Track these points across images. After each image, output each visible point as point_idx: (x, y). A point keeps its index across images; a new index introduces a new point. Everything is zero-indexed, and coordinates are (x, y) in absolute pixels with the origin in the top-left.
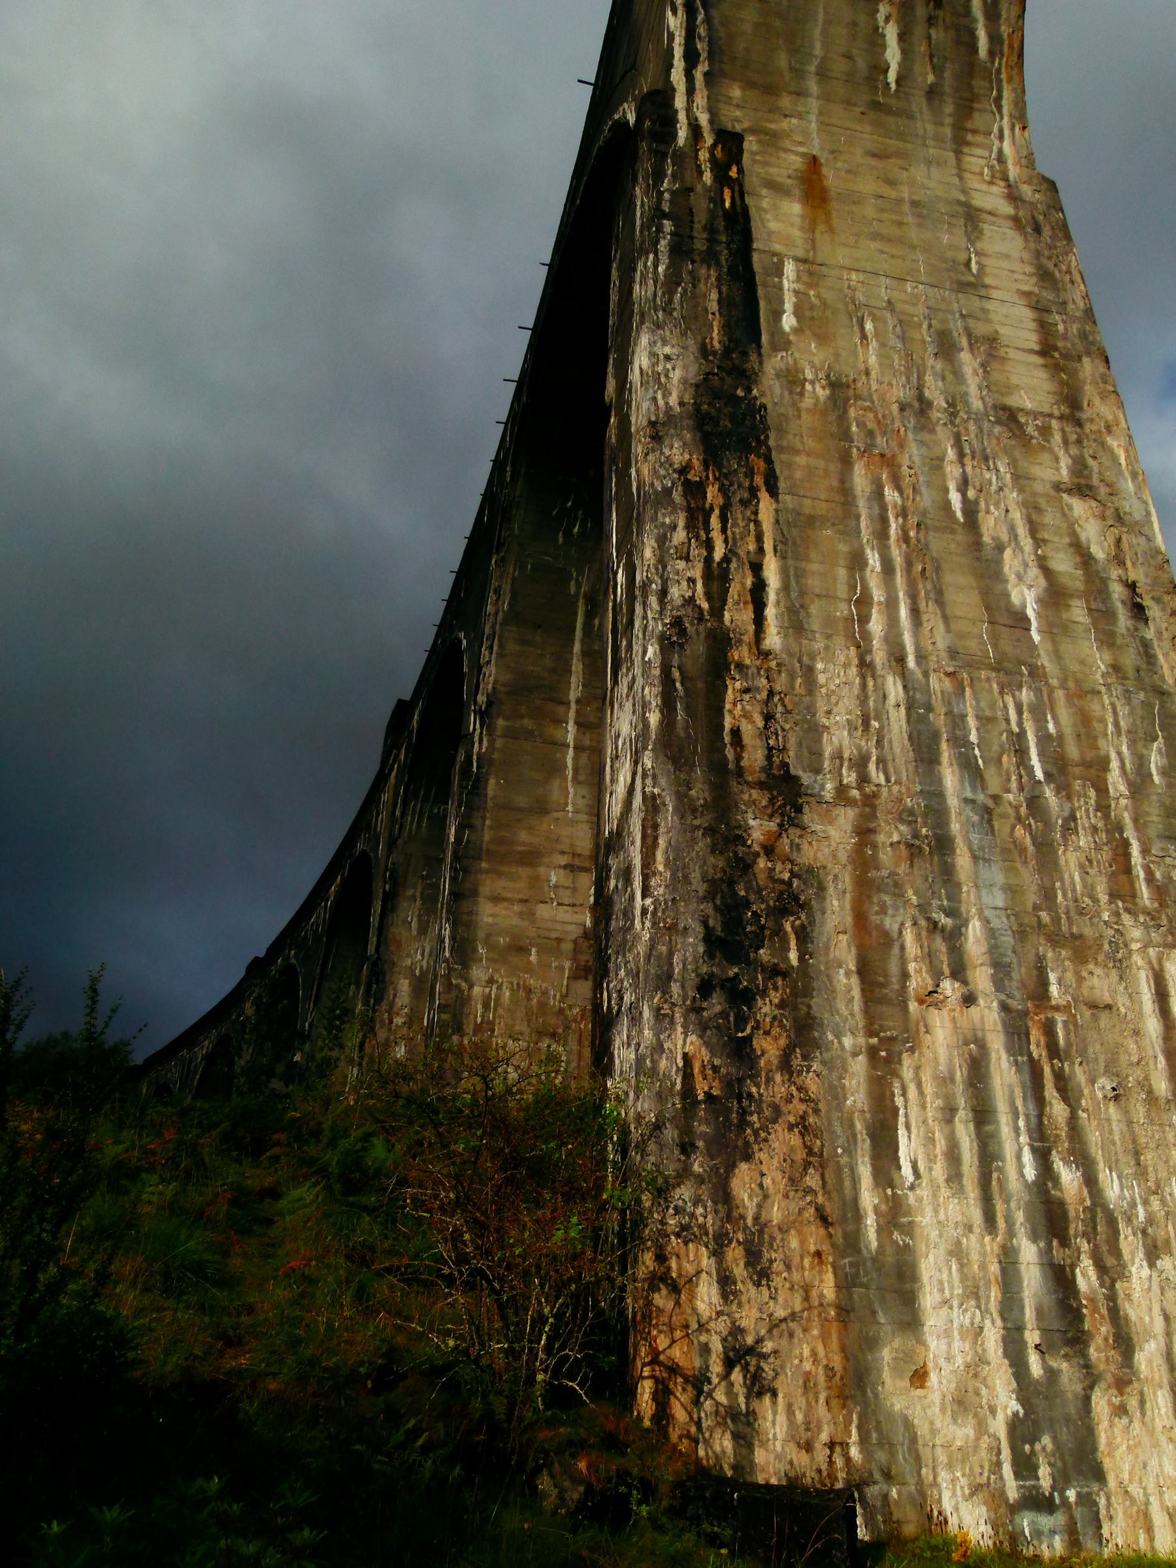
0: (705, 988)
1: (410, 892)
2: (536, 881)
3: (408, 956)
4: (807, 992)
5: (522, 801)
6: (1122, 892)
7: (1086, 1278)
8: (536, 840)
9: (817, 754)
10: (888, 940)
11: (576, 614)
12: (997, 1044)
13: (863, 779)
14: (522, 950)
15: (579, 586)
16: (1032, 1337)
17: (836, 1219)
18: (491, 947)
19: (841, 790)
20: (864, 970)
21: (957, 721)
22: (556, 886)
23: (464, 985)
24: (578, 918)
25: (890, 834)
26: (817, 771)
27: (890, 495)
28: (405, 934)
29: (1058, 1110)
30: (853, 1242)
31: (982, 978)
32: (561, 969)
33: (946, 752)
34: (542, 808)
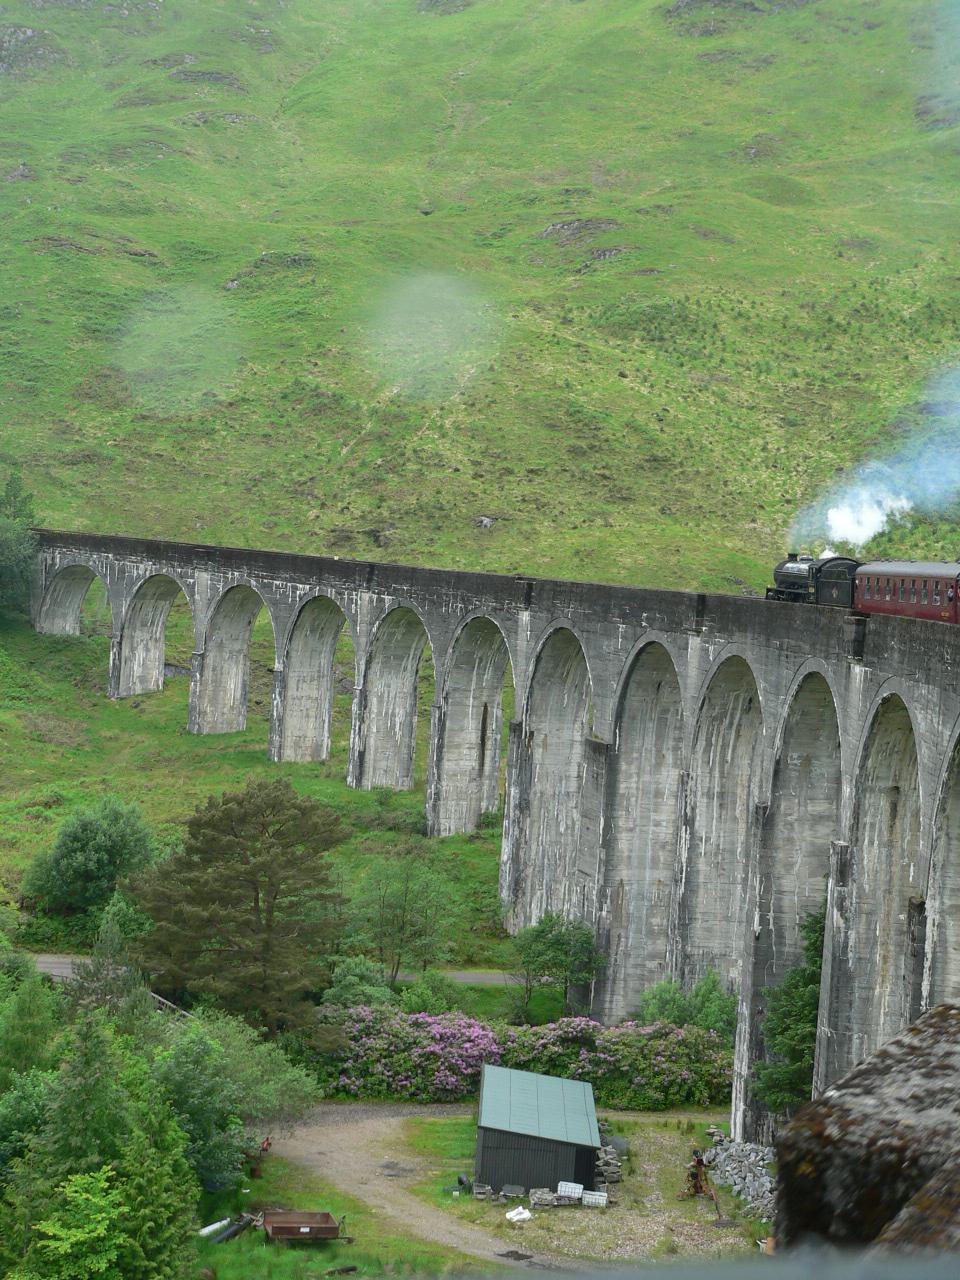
6: (564, 875)
17: (525, 913)
34: (462, 729)
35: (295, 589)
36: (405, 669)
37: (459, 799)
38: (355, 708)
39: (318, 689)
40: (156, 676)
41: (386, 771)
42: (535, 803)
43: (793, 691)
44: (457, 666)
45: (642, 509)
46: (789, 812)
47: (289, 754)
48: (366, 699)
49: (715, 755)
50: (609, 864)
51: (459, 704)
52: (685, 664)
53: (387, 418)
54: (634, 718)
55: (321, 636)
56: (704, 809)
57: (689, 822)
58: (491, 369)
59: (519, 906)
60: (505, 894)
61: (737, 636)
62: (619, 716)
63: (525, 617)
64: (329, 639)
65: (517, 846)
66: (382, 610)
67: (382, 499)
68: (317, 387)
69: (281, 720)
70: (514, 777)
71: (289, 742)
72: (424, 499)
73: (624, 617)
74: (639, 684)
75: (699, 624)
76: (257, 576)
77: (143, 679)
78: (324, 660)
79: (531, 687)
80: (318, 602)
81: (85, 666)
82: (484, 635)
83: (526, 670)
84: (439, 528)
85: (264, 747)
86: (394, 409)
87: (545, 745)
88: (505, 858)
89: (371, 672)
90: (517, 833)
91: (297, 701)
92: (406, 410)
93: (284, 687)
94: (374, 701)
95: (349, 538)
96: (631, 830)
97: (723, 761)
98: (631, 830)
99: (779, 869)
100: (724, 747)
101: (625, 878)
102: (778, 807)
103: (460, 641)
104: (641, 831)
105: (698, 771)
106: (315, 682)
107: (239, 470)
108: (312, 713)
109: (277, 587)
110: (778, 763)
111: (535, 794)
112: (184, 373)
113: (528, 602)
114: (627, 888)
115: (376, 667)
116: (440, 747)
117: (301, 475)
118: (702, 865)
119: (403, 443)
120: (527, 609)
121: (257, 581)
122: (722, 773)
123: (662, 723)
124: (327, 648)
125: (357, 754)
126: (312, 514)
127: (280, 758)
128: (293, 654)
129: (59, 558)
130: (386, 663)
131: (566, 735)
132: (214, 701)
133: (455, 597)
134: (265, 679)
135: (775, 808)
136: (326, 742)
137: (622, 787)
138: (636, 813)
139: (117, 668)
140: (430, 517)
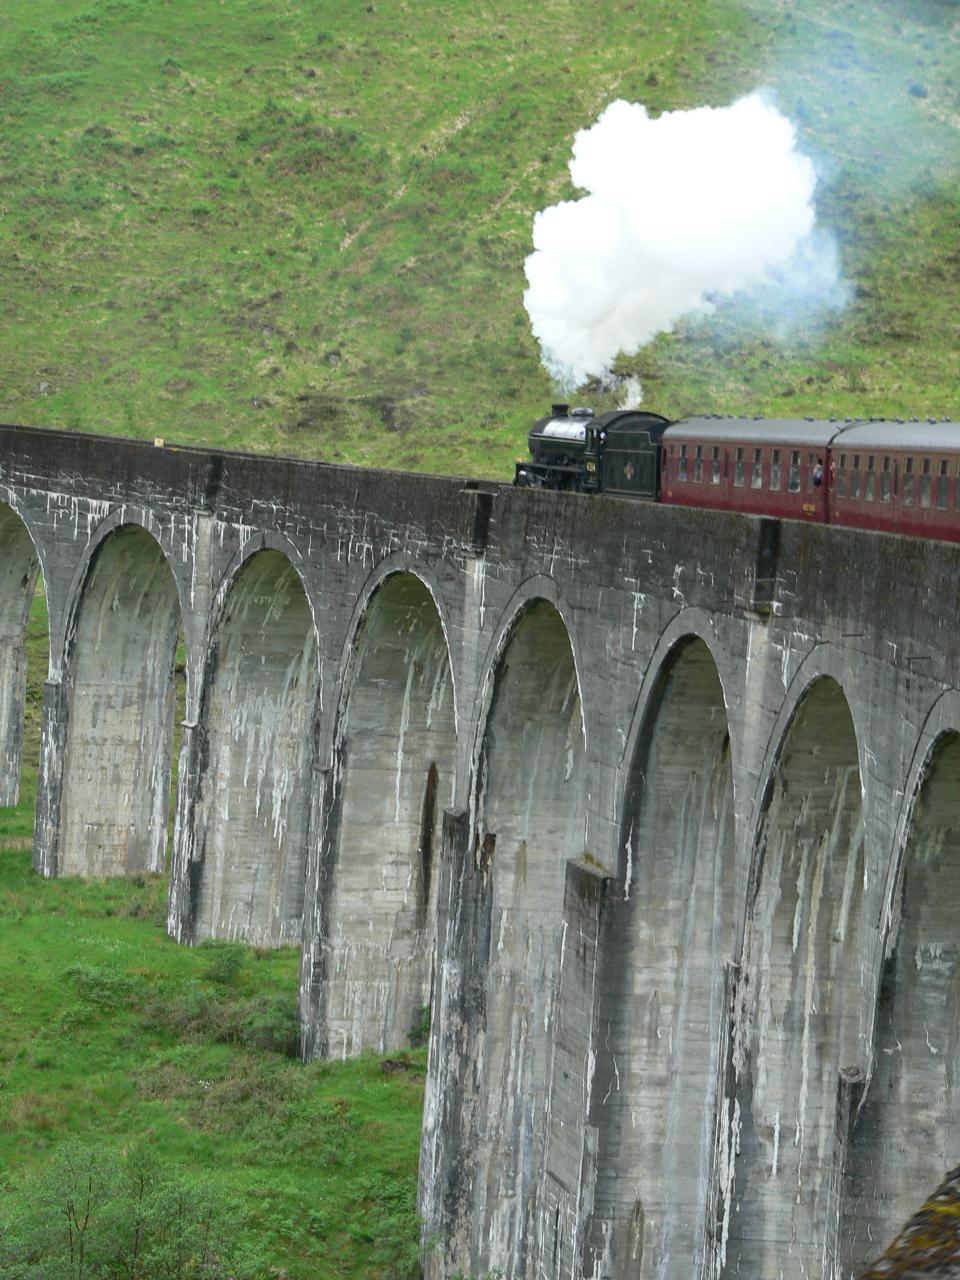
0: (448, 1196)
1: (229, 665)
2: (372, 875)
3: (229, 722)
4: (472, 1196)
5: (365, 817)
7: (529, 1260)
8: (373, 845)
9: (485, 1126)
10: (496, 1181)
11: (407, 675)
12: (519, 1207)
13: (497, 1132)
14: (363, 923)
15: (410, 657)
16: (513, 1273)
17: (473, 1252)
18: (345, 923)
19: (491, 1137)
20: (489, 1188)
21: (529, 1110)
22: (386, 878)
23: (329, 949)
24: (400, 898)
25: (501, 1150)
26: (484, 1132)
27: (524, 1024)
28: (224, 702)
29: (531, 1222)
30: (476, 1254)
31: (519, 1190)
32: (388, 933)
33: (523, 1122)
34: (378, 822)
35: (85, 508)
36: (294, 683)
37: (370, 976)
39: (140, 723)
41: (250, 905)
42: (498, 998)
43: (915, 781)
44: (363, 680)
45: (931, 356)
46: (919, 1099)
47: (76, 860)
48: (205, 749)
49: (805, 920)
50: (606, 1164)
51: (374, 764)
52: (740, 694)
53: (439, 179)
54: (668, 816)
55: (146, 610)
56: (777, 1057)
57: (738, 1087)
58: (652, 81)
59: (460, 1235)
60: (428, 1208)
61: (830, 628)
62: (632, 811)
63: (476, 571)
65: (455, 1095)
66: (235, 554)
67: (407, 336)
68: (308, 118)
69: (58, 789)
70: (449, 939)
71: (75, 834)
72: (491, 336)
73: (642, 572)
74: (678, 734)
75: (764, 593)
76: (20, 482)
79: (488, 733)
80: (125, 536)
82: (409, 609)
83: (477, 695)
84: (512, 394)
85: (29, 843)
86: (453, 159)
87: (521, 865)
88: (429, 1121)
89: (217, 690)
90: (454, 1065)
91: (93, 749)
92: (474, 163)
93: (66, 718)
94: (223, 753)
95: (332, 413)
96: (662, 1083)
97: (826, 937)
98: (662, 1083)
100: (829, 902)
101: (647, 1199)
102: (893, 1085)
103: (369, 626)
104: (686, 1086)
105: (764, 961)
106: (134, 709)
107: (138, 279)
108: (127, 774)
109: (54, 505)
110: (889, 967)
111: (498, 976)
112: (53, 90)
113: (481, 537)
114: (651, 1222)
115: (228, 679)
116: (329, 861)
117: (256, 288)
118: (772, 1198)
119: (460, 226)
120: (479, 555)
121: (19, 493)
122: (823, 967)
125: (185, 868)
126: (265, 366)
127: (55, 866)
128: (84, 648)
130: (249, 670)
133: (358, 526)
135: (885, 1090)
137: (641, 981)
138: (673, 1041)
140: (498, 371)
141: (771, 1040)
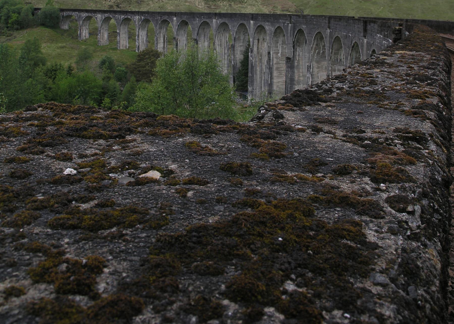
38: (137, 38)
40: (87, 35)
62: (198, 34)
63: (175, 19)
64: (127, 26)
69: (119, 41)
71: (121, 45)
73: (198, 17)
77: (85, 36)
78: (126, 30)
81: (73, 34)
94: (140, 36)
99: (236, 54)
113: (175, 16)
115: (140, 30)
116: (157, 43)
123: (205, 35)
124: (127, 28)
129: (65, 14)
131: (183, 39)
132: (103, 39)
134: (113, 35)
136: (128, 45)
139: (80, 34)
141: (217, 46)
